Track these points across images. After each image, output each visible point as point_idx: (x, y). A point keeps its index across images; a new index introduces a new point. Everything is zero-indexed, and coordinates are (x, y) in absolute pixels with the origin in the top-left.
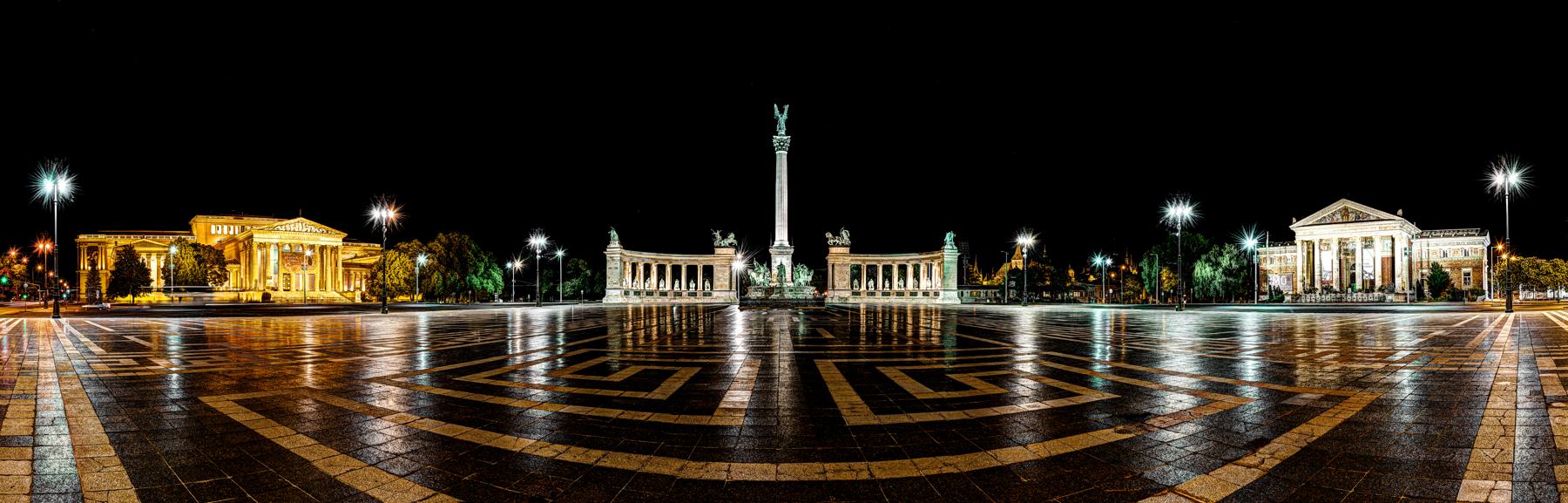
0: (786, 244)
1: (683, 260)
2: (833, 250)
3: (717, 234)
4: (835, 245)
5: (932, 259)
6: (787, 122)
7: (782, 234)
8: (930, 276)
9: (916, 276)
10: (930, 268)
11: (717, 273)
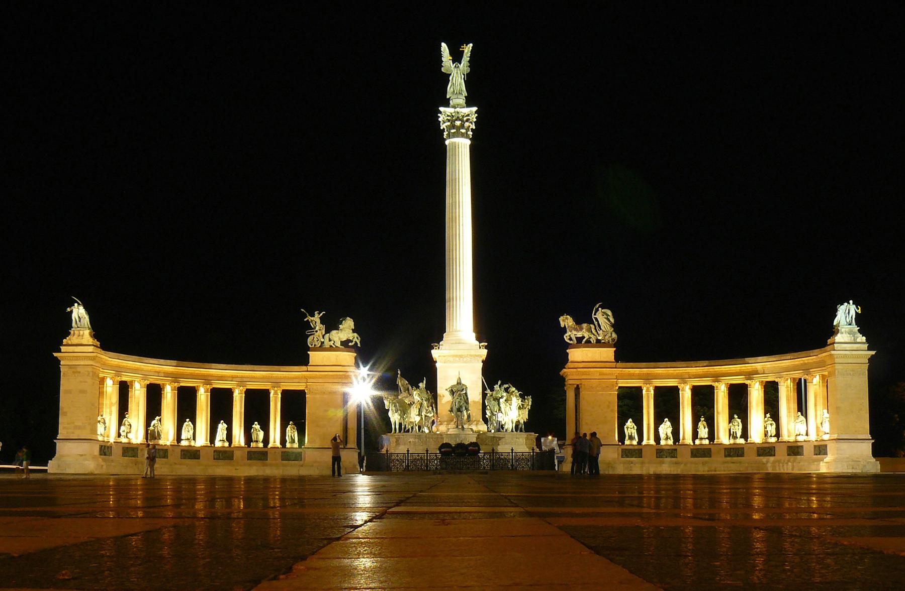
1: (239, 379)
3: (316, 319)
5: (807, 369)
6: (470, 81)
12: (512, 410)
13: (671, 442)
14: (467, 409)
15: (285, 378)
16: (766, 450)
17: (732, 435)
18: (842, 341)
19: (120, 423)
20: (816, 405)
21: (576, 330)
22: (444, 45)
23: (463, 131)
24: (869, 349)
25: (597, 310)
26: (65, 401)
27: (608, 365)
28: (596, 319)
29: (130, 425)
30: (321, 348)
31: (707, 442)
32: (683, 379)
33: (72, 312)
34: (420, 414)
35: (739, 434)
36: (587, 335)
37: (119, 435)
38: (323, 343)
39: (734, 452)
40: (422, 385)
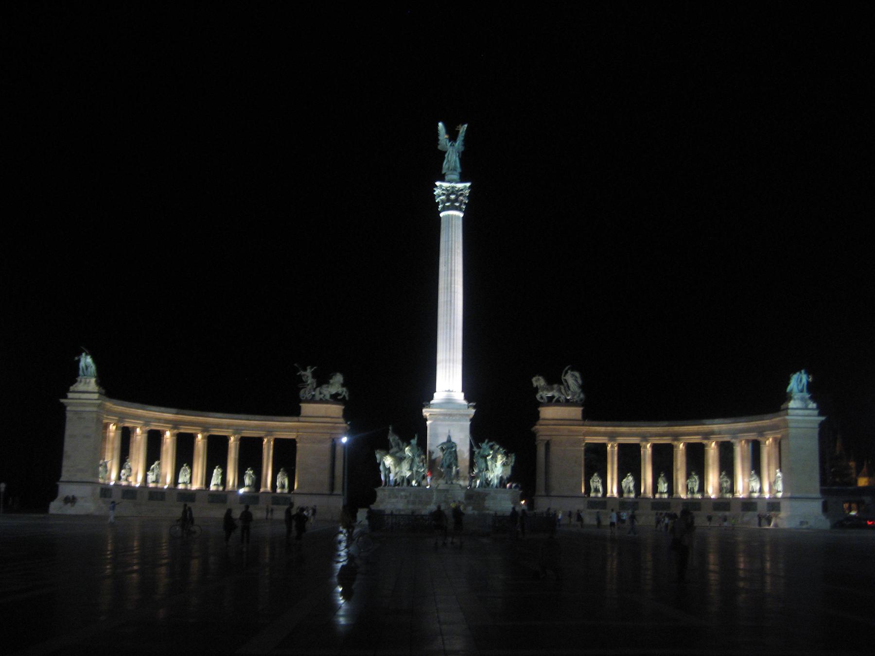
0: (459, 396)
1: (234, 427)
3: (308, 374)
4: (551, 401)
5: (761, 431)
7: (449, 380)
8: (756, 467)
9: (727, 468)
11: (301, 457)
12: (497, 468)
13: (632, 495)
14: (457, 466)
15: (278, 427)
16: (722, 504)
17: (688, 489)
19: (121, 466)
20: (769, 465)
21: (548, 390)
22: (440, 124)
23: (457, 204)
24: (820, 414)
25: (566, 372)
27: (575, 422)
28: (566, 381)
29: (130, 469)
30: (312, 400)
31: (665, 496)
32: (645, 438)
33: (79, 361)
34: (411, 469)
35: (696, 489)
36: (557, 395)
37: (119, 478)
38: (314, 395)
40: (414, 442)
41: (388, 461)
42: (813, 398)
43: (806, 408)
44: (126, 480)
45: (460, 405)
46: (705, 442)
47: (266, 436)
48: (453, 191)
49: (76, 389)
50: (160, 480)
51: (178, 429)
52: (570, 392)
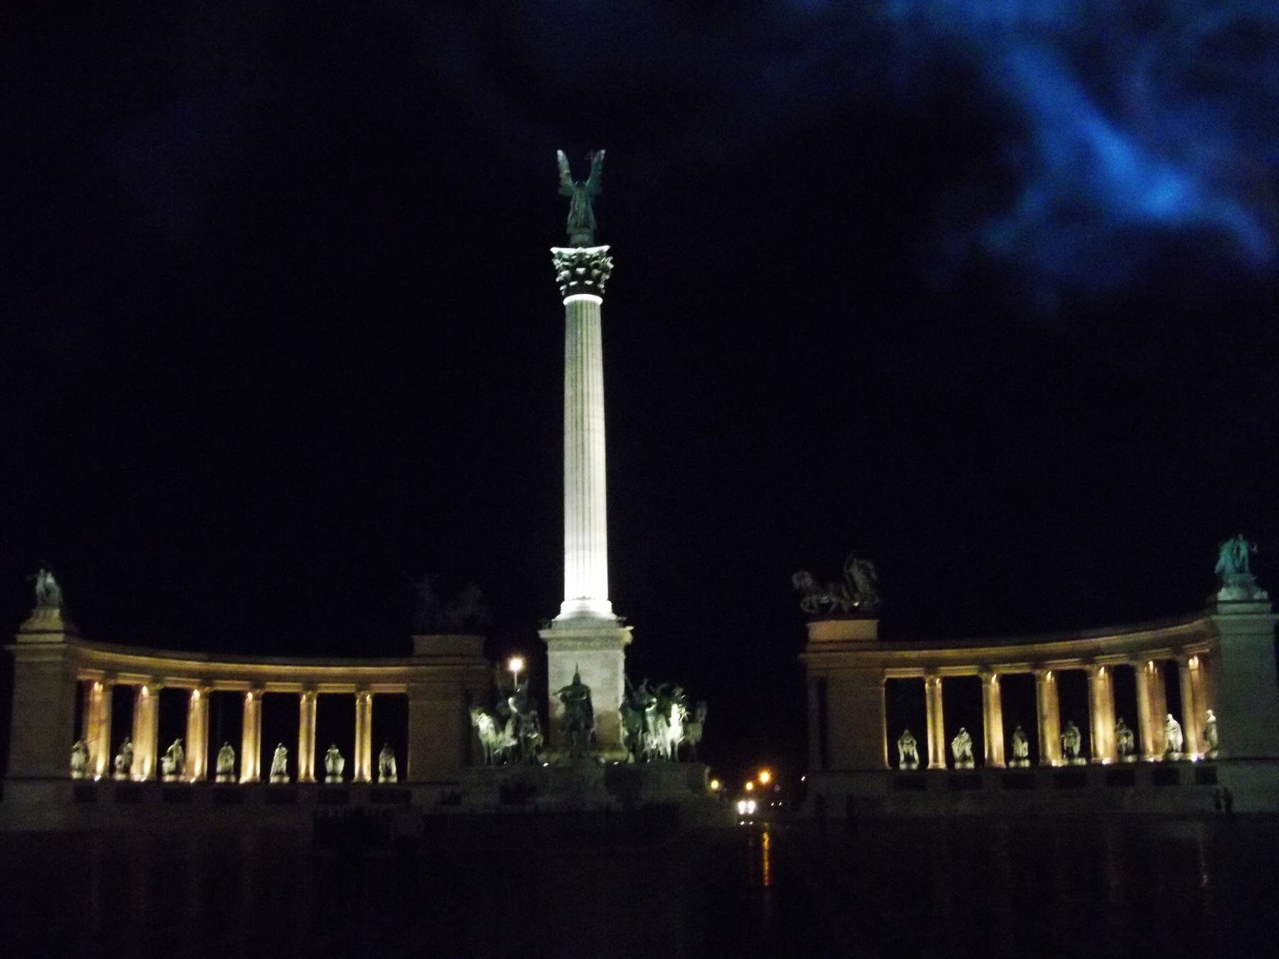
0: (603, 608)
2: (822, 630)
4: (826, 613)
6: (600, 205)
7: (586, 580)
10: (1171, 676)
13: (971, 765)
16: (1119, 774)
17: (1067, 752)
18: (1229, 598)
23: (589, 283)
26: (20, 717)
29: (131, 754)
31: (1026, 763)
33: (35, 582)
34: (515, 735)
35: (1077, 749)
37: (111, 768)
39: (1068, 776)
41: (484, 723)
42: (1261, 584)
43: (1253, 601)
44: (126, 770)
45: (603, 623)
46: (1088, 667)
47: (359, 690)
48: (581, 261)
49: (29, 627)
50: (184, 770)
51: (211, 685)
52: (856, 595)
